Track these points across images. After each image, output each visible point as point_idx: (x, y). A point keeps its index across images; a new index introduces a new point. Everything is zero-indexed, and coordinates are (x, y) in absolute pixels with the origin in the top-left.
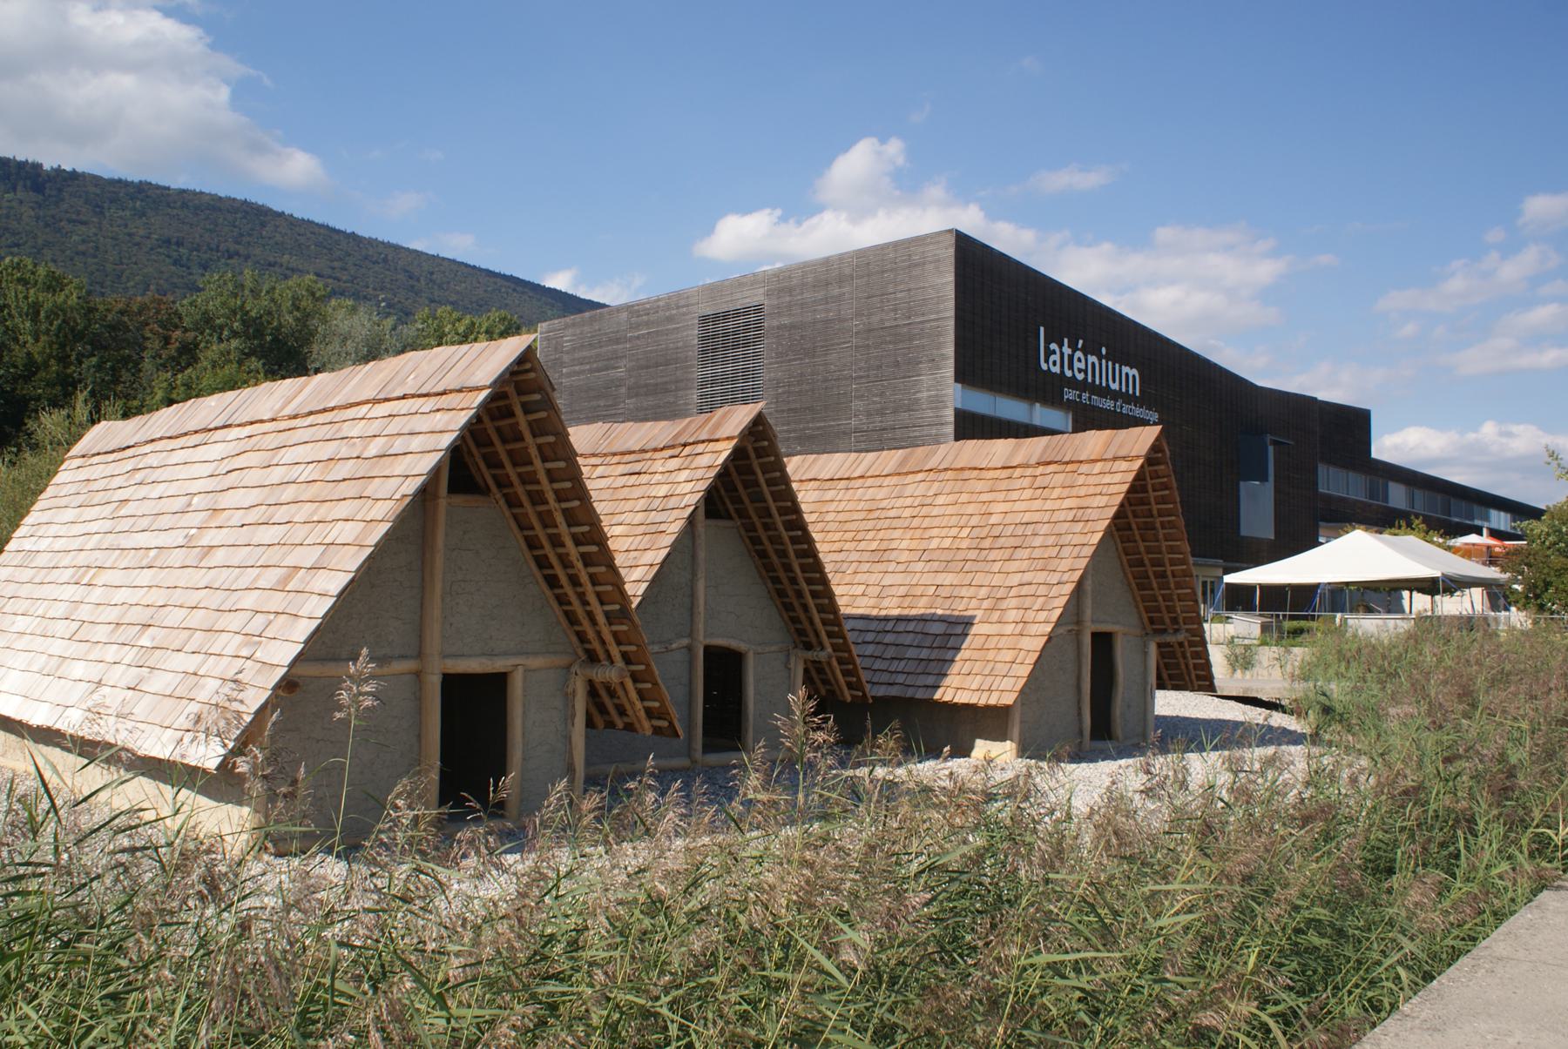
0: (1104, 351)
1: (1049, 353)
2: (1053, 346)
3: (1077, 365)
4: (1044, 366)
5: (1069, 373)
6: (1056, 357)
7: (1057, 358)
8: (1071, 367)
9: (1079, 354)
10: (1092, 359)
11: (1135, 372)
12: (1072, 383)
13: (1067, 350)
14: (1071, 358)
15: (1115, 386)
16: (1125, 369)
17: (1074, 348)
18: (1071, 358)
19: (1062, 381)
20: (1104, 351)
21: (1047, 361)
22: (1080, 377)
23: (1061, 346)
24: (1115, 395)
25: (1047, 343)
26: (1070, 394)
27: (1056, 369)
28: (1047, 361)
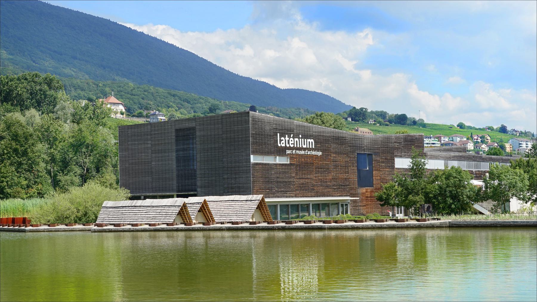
0: (300, 136)
1: (281, 140)
2: (282, 138)
3: (291, 142)
4: (279, 145)
5: (288, 146)
6: (284, 142)
7: (283, 142)
8: (289, 143)
9: (292, 139)
10: (296, 139)
11: (312, 140)
12: (290, 148)
13: (287, 139)
14: (289, 141)
15: (305, 146)
16: (308, 140)
17: (289, 137)
18: (289, 141)
19: (286, 148)
20: (300, 136)
21: (280, 143)
22: (292, 146)
23: (285, 137)
24: (305, 149)
25: (280, 137)
26: (288, 152)
27: (284, 145)
28: (280, 143)
